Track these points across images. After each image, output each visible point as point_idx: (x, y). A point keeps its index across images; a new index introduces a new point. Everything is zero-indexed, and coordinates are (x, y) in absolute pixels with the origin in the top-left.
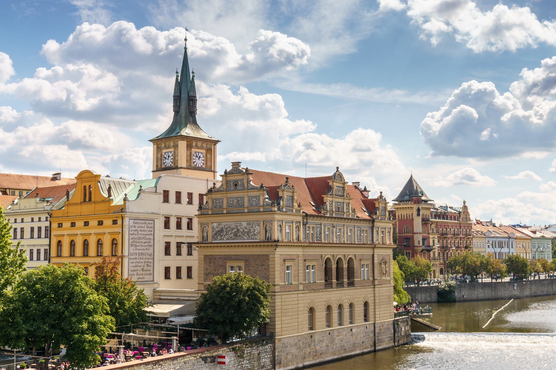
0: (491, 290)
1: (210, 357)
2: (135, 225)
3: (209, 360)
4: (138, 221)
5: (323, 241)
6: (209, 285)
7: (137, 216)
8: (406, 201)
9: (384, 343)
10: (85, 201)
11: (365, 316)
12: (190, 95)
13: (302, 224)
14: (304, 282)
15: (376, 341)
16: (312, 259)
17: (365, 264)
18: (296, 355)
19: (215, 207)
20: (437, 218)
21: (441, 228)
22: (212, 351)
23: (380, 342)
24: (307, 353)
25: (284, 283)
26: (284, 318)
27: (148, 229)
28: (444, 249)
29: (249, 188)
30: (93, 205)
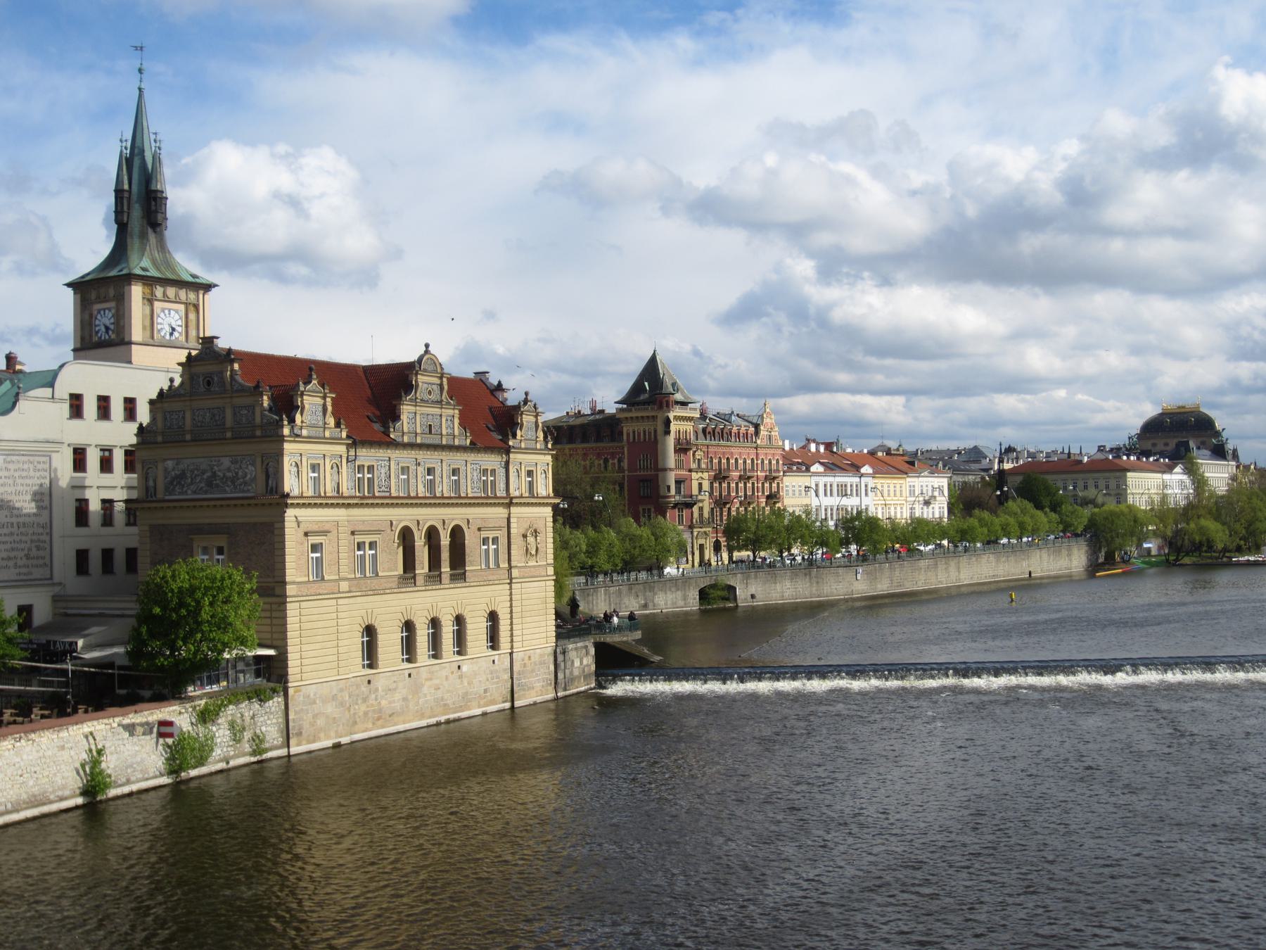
1: (142, 725)
2: (6, 465)
3: (139, 730)
4: (14, 458)
5: (394, 493)
9: (533, 693)
13: (344, 461)
17: (491, 537)
19: (170, 428)
20: (708, 437)
22: (146, 713)
23: (524, 690)
24: (361, 714)
25: (306, 579)
26: (305, 647)
27: (38, 474)
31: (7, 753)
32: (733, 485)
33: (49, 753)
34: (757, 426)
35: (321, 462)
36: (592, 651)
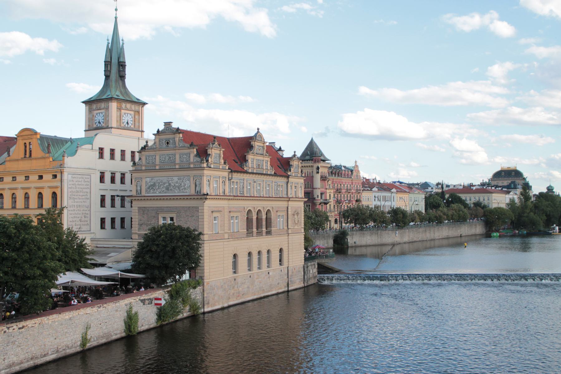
0: (378, 237)
1: (148, 299)
2: (72, 179)
3: (147, 302)
6: (146, 234)
7: (75, 171)
8: (307, 160)
10: (25, 157)
11: (280, 261)
12: (120, 61)
13: (227, 179)
14: (229, 232)
15: (289, 283)
16: (235, 210)
18: (222, 296)
20: (333, 175)
21: (346, 184)
22: (150, 294)
23: (292, 283)
24: (231, 294)
25: (212, 233)
27: (85, 183)
28: (338, 202)
29: (181, 146)
30: (34, 161)
31: (95, 314)
32: (343, 196)
33: (112, 313)
34: (352, 171)
35: (218, 180)
36: (316, 266)
